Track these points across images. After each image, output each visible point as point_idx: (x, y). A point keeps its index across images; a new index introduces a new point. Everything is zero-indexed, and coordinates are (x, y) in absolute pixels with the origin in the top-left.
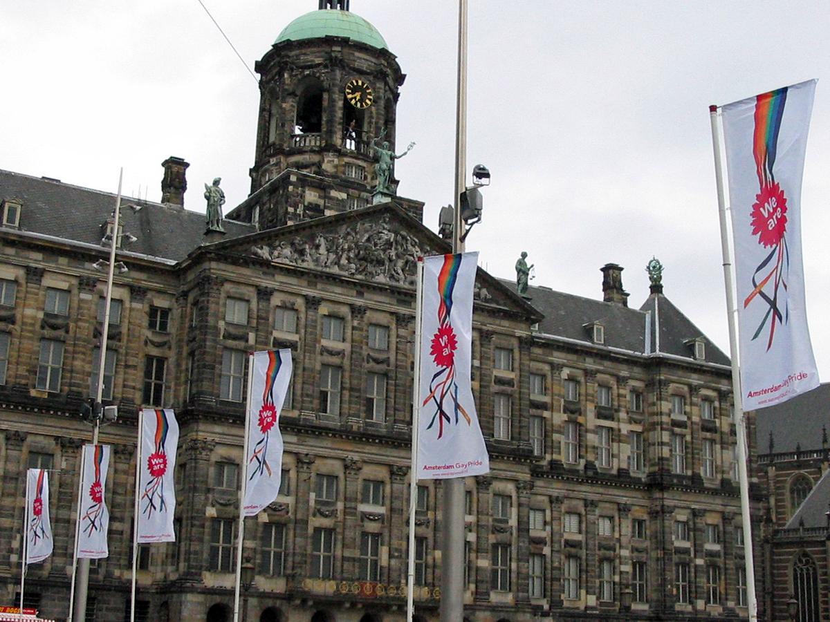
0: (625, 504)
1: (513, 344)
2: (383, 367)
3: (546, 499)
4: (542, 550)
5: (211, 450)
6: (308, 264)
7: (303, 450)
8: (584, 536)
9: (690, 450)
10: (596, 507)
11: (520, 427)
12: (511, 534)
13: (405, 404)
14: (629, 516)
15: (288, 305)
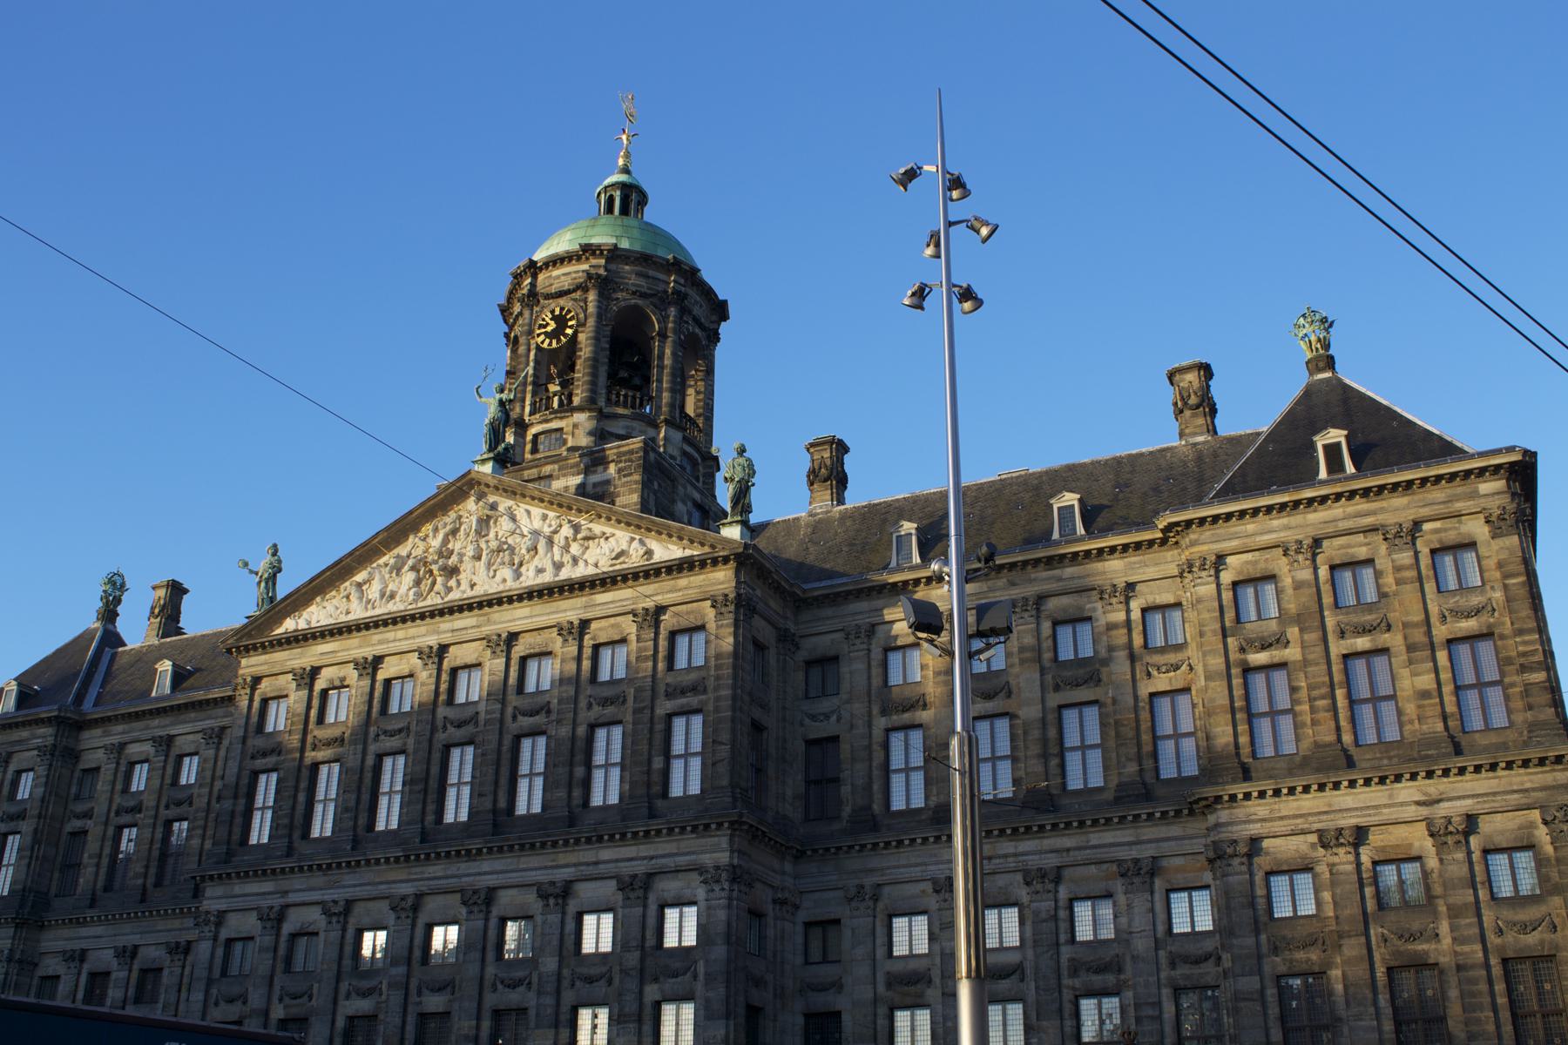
0: (1136, 861)
1: (703, 616)
2: (470, 729)
3: (928, 887)
4: (921, 995)
5: (219, 924)
6: (358, 612)
7: (328, 895)
8: (1030, 953)
9: (1303, 694)
10: (1058, 880)
11: (714, 764)
12: (695, 977)
13: (496, 783)
14: (1159, 884)
15: (337, 683)
